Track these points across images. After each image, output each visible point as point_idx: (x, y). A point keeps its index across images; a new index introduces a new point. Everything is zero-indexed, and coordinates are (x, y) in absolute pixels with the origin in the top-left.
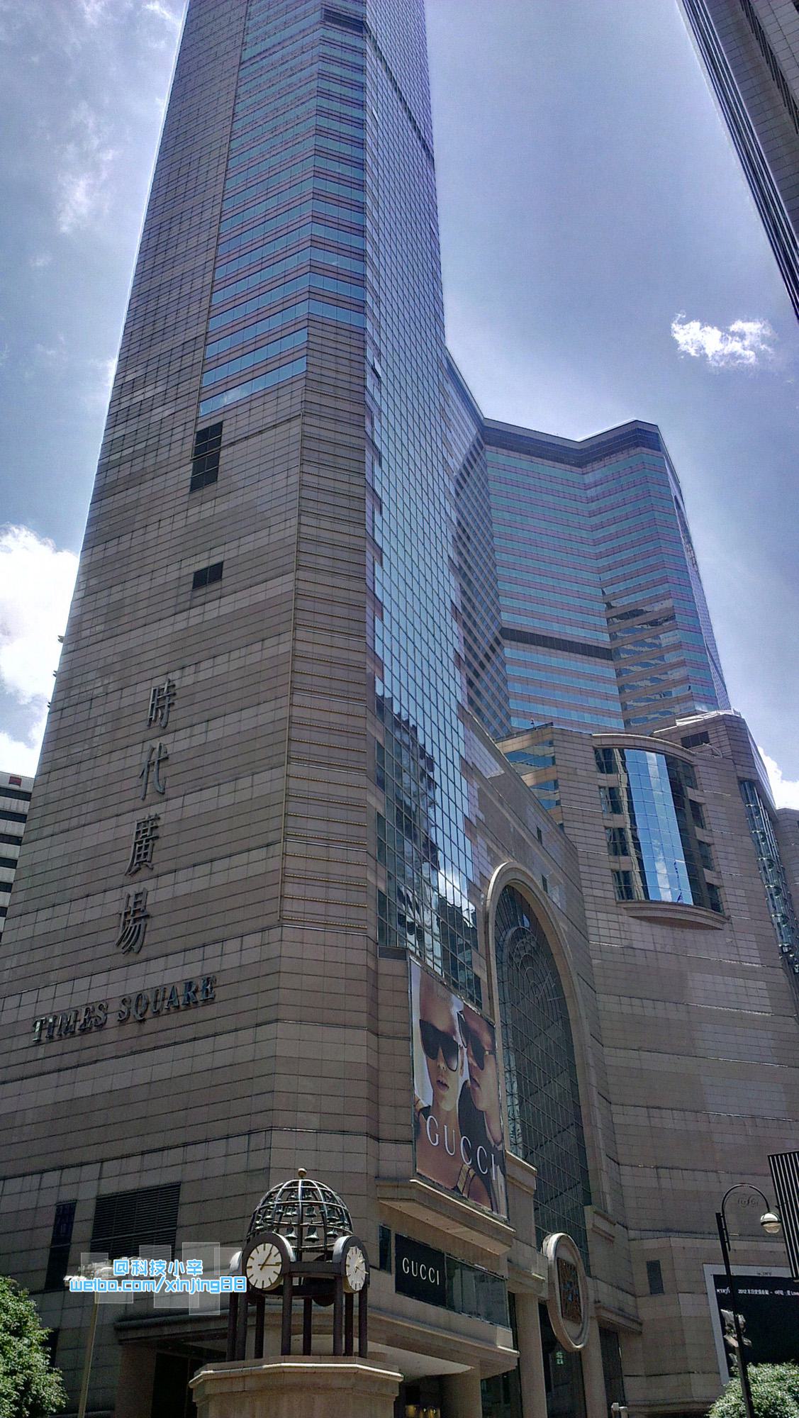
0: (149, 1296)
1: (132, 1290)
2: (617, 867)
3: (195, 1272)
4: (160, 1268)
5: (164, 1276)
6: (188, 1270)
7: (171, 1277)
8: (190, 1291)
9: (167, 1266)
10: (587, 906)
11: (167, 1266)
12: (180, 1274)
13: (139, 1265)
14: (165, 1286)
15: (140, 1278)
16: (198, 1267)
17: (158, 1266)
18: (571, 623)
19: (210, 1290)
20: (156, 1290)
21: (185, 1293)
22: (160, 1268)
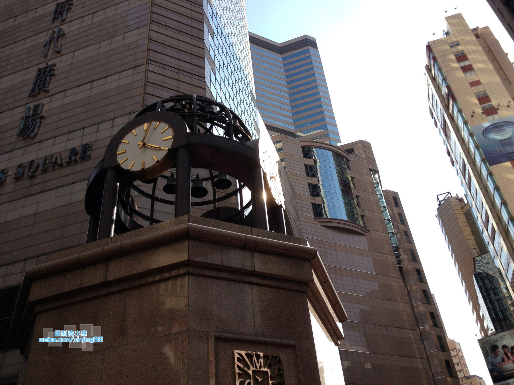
0: (67, 344)
1: (61, 341)
2: (314, 202)
3: (84, 335)
4: (72, 334)
5: (73, 336)
6: (82, 334)
7: (76, 337)
8: (82, 342)
9: (74, 333)
10: (300, 219)
11: (74, 333)
12: (79, 336)
13: (64, 333)
14: (73, 340)
15: (65, 337)
16: (85, 333)
17: (71, 333)
18: (277, 120)
19: (90, 342)
20: (70, 341)
21: (81, 343)
22: (72, 334)
